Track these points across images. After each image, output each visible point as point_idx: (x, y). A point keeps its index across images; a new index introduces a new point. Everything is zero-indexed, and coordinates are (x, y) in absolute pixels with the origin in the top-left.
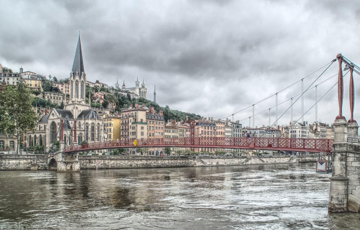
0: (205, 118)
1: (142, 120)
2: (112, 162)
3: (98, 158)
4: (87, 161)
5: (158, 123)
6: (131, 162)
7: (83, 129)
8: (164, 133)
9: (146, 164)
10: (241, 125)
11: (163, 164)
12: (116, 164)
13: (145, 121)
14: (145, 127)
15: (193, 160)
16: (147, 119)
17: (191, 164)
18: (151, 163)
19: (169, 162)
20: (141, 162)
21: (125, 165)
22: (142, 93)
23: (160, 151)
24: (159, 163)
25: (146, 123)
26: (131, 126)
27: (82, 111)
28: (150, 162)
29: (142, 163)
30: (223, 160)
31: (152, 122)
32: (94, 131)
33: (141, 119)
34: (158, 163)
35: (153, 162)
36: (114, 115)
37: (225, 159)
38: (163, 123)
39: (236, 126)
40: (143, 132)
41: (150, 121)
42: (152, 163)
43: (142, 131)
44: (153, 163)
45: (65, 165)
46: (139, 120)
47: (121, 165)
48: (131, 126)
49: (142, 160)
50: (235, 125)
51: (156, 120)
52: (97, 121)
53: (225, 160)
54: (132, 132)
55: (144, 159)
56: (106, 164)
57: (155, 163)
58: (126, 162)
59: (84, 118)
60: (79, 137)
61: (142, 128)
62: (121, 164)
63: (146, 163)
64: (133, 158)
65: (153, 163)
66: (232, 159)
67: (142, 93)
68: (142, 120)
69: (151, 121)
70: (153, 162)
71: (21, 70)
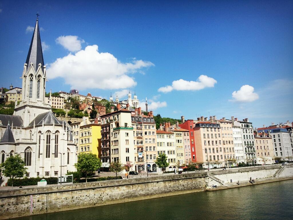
0: (205, 118)
1: (126, 124)
2: (65, 195)
3: (36, 193)
4: (13, 200)
5: (147, 127)
6: (100, 193)
7: (34, 141)
9: (128, 193)
10: (251, 123)
11: (156, 190)
12: (71, 199)
14: (130, 132)
16: (132, 122)
17: (200, 185)
18: (137, 190)
19: (165, 186)
20: (118, 190)
21: (88, 199)
22: (135, 104)
23: (153, 164)
24: (150, 189)
25: (132, 128)
26: (112, 133)
27: (36, 116)
28: (134, 189)
29: (120, 192)
32: (49, 143)
34: (148, 190)
35: (139, 188)
36: (93, 122)
38: (153, 126)
39: (245, 125)
40: (128, 140)
42: (138, 190)
43: (127, 138)
44: (139, 191)
46: (122, 125)
48: (112, 133)
49: (120, 187)
50: (244, 124)
51: (144, 123)
54: (114, 141)
55: (123, 185)
56: (51, 202)
57: (143, 191)
58: (92, 192)
59: (36, 124)
60: (25, 153)
63: (127, 191)
64: (103, 186)
65: (139, 191)
67: (135, 104)
68: (126, 124)
70: (139, 188)
71: (11, 87)
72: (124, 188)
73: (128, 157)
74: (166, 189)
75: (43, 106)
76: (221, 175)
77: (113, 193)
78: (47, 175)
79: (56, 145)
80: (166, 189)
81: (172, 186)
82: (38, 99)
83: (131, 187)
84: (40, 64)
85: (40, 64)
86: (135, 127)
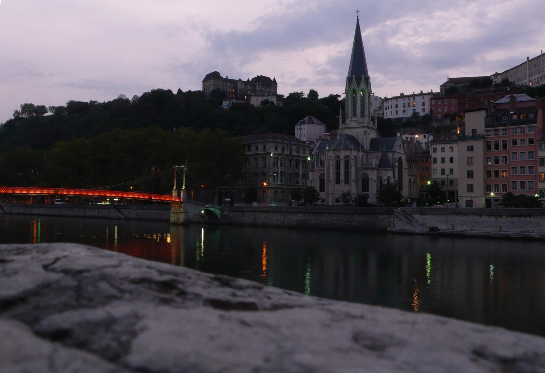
1: (474, 131)
5: (519, 131)
8: (536, 153)
13: (484, 133)
15: (386, 216)
16: (487, 126)
30: (493, 219)
31: (500, 132)
33: (473, 130)
35: (314, 217)
37: (501, 216)
41: (495, 130)
45: (174, 216)
47: (272, 220)
52: (355, 153)
53: (499, 219)
61: (471, 149)
62: (272, 219)
66: (527, 219)
68: (474, 131)
69: (497, 130)
72: (301, 215)
73: (472, 185)
74: (338, 222)
75: (357, 125)
76: (436, 216)
77: (293, 218)
78: (338, 202)
79: (338, 170)
80: (338, 222)
81: (345, 220)
82: (354, 119)
83: (307, 215)
84: (354, 76)
85: (354, 76)
86: (492, 133)
